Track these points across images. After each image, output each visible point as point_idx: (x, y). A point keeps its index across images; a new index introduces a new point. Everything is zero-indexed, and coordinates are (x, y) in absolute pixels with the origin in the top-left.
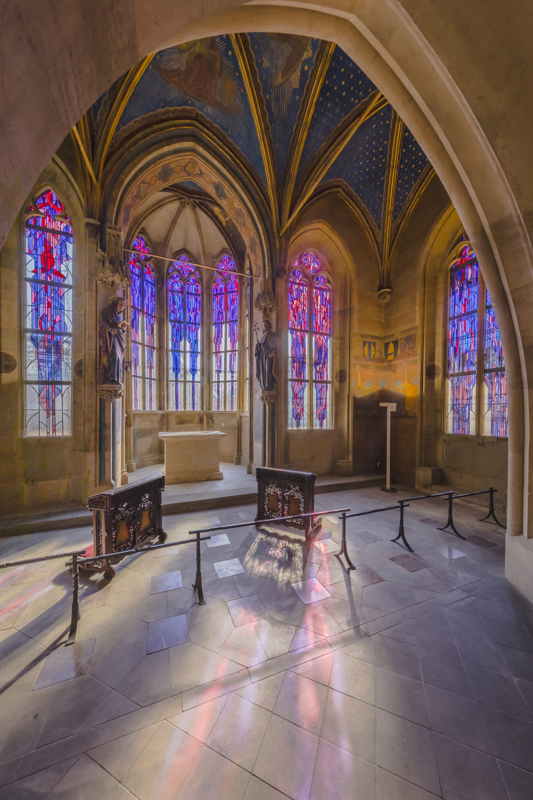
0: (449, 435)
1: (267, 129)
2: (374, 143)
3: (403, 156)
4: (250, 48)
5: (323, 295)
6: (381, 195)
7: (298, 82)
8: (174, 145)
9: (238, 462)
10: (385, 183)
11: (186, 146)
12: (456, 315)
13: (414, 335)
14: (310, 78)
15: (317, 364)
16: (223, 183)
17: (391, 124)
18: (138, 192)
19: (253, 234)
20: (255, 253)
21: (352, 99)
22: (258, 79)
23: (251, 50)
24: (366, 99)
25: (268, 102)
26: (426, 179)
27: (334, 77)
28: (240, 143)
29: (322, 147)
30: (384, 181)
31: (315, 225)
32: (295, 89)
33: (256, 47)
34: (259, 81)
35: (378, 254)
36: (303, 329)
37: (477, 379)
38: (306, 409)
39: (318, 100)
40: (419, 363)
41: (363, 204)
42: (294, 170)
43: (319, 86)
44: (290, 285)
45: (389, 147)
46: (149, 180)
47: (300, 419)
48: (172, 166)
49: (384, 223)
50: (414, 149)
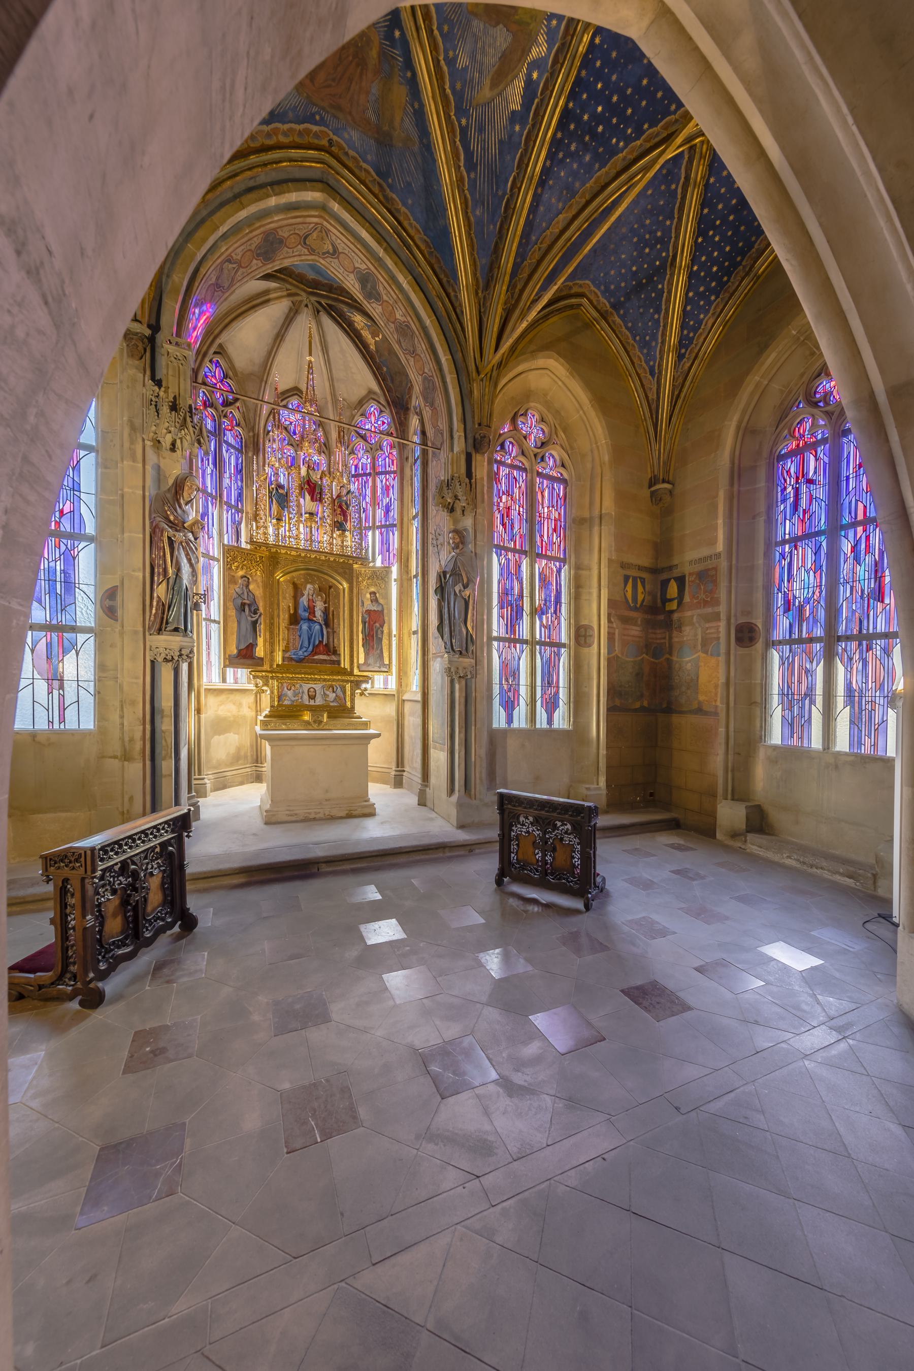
1: (460, 180)
2: (648, 222)
3: (697, 249)
4: (435, 28)
6: (656, 316)
7: (519, 99)
8: (287, 195)
9: (398, 782)
11: (309, 199)
14: (541, 94)
16: (376, 272)
17: (679, 190)
18: (217, 279)
19: (430, 370)
21: (614, 140)
22: (447, 86)
23: (436, 32)
24: (638, 143)
25: (464, 131)
27: (585, 96)
28: (410, 202)
29: (558, 223)
30: (662, 290)
31: (541, 362)
32: (513, 112)
33: (446, 28)
34: (448, 91)
39: (554, 134)
41: (624, 329)
42: (508, 260)
44: (495, 466)
45: (673, 231)
49: (660, 365)
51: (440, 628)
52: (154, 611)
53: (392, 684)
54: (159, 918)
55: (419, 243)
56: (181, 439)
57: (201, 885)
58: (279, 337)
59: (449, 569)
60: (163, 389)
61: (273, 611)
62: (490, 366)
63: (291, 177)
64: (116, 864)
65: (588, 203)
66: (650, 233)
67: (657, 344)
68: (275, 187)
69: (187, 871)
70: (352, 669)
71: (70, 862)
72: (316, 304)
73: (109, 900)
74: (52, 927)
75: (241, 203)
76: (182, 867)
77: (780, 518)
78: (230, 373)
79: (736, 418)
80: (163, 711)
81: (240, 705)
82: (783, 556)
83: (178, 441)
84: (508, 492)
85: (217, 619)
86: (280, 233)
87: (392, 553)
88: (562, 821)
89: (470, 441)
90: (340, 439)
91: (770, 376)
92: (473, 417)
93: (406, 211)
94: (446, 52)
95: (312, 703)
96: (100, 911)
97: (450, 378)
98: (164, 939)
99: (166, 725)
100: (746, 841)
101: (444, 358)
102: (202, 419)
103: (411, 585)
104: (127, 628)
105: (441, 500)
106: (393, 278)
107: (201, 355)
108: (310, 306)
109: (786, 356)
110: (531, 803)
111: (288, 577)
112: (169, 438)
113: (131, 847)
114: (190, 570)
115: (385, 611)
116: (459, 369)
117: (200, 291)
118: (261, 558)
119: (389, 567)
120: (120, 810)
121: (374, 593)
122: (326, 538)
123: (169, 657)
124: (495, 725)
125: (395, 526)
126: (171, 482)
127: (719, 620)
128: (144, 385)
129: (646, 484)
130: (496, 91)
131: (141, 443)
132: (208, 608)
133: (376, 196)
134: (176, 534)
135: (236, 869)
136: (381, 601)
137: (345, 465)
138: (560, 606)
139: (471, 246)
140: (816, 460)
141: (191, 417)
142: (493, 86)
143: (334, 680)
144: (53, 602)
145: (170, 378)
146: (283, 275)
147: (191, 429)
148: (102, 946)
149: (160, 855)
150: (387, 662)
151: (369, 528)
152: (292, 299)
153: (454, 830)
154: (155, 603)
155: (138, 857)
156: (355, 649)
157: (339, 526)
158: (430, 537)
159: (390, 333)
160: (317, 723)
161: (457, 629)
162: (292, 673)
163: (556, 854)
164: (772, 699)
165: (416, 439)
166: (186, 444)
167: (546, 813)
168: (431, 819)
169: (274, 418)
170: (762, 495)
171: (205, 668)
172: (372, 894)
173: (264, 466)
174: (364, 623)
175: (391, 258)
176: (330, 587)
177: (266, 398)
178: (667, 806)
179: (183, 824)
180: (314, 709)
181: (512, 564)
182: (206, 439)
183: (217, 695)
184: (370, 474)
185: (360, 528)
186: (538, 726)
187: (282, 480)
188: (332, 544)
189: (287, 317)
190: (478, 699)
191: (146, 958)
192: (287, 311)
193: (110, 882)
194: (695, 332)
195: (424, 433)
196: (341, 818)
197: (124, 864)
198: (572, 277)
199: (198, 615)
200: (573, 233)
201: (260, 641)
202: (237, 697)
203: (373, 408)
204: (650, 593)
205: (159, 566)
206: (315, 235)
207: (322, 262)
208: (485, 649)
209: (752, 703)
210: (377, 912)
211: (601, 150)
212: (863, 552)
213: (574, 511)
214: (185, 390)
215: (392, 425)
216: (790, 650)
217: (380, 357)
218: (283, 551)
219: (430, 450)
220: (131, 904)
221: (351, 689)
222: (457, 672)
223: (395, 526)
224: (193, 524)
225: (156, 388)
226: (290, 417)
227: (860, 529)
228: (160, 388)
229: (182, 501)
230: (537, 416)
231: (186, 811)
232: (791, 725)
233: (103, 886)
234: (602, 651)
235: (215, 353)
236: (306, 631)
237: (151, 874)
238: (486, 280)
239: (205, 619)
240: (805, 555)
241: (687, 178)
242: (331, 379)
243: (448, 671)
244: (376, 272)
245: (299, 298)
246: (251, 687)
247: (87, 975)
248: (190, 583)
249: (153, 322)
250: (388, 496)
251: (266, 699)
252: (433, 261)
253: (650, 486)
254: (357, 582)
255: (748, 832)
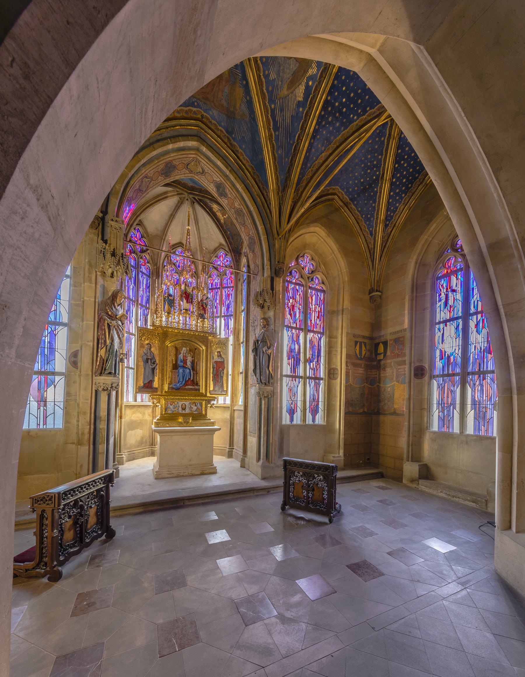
0: (435, 433)
1: (271, 136)
2: (369, 156)
3: (395, 171)
5: (318, 295)
6: (374, 205)
7: (302, 95)
8: (178, 143)
9: (230, 455)
10: (378, 194)
12: (442, 320)
13: (404, 337)
15: (310, 361)
16: (225, 183)
17: (386, 141)
18: (140, 186)
20: (253, 252)
21: (352, 116)
22: (264, 89)
24: (364, 117)
25: (273, 111)
26: (416, 193)
27: (336, 94)
28: (244, 146)
29: (322, 157)
31: (312, 229)
32: (299, 102)
34: (265, 91)
35: (369, 259)
36: (298, 327)
37: (461, 381)
38: (299, 404)
39: (320, 113)
40: (407, 362)
41: (356, 211)
43: (322, 101)
44: (287, 284)
45: (383, 161)
46: (151, 175)
47: (294, 413)
48: (176, 163)
49: (375, 230)
50: (405, 165)
51: (255, 371)
52: (98, 363)
53: (228, 401)
54: (94, 531)
55: (248, 167)
56: (117, 271)
57: (119, 513)
58: (172, 216)
59: (260, 339)
60: (108, 245)
61: (164, 362)
62: (285, 231)
63: (181, 134)
64: (72, 502)
65: (338, 147)
66: (370, 162)
67: (374, 219)
68: (172, 139)
69: (111, 506)
70: (206, 393)
71: (46, 501)
72: (193, 199)
73: (66, 521)
74: (35, 538)
75: (154, 148)
76: (108, 503)
77: (438, 310)
78: (145, 235)
79: (415, 258)
80: (101, 418)
81: (144, 414)
82: (439, 330)
83: (115, 272)
84: (293, 297)
85: (133, 367)
86: (174, 163)
87: (228, 330)
88: (318, 474)
89: (273, 271)
90: (203, 270)
91: (433, 235)
92: (275, 258)
93: (242, 151)
94: (264, 71)
95: (184, 412)
96: (61, 528)
97: (263, 238)
98: (97, 542)
99: (102, 425)
100: (418, 484)
101: (260, 227)
102: (128, 261)
103: (240, 348)
104: (83, 373)
105: (257, 302)
106: (234, 186)
107: (130, 226)
108: (189, 200)
109: (441, 225)
110: (301, 465)
111: (173, 344)
112: (110, 271)
113: (80, 492)
114: (119, 341)
115: (225, 362)
116: (269, 233)
117: (130, 193)
118: (158, 333)
119: (228, 338)
120: (75, 472)
121: (219, 352)
122: (194, 322)
123: (105, 388)
124: (284, 423)
125: (232, 315)
126: (110, 294)
127: (405, 364)
128: (98, 243)
129: (367, 292)
130: (290, 91)
131: (95, 273)
132: (128, 361)
133: (225, 143)
134: (112, 322)
135: (138, 504)
136: (223, 356)
137: (206, 284)
138: (320, 358)
139: (276, 169)
140: (457, 279)
141: (123, 259)
142: (289, 88)
143: (196, 399)
144: (43, 359)
145: (112, 239)
146: (176, 184)
147: (122, 266)
148: (62, 547)
149: (96, 496)
150: (225, 389)
151: (218, 317)
152: (179, 196)
153: (260, 480)
154: (99, 359)
155: (84, 498)
156: (208, 381)
157: (202, 316)
158: (251, 321)
159: (231, 214)
160: (187, 423)
161: (264, 371)
162: (173, 396)
163: (314, 492)
164: (433, 406)
165: (245, 269)
166: (119, 274)
167: (309, 470)
168: (248, 475)
169: (168, 259)
170: (428, 299)
171: (125, 394)
172: (213, 516)
173: (162, 284)
174: (213, 368)
175: (233, 176)
176: (196, 349)
177: (164, 249)
178: (376, 465)
179: (109, 479)
180: (184, 415)
181: (294, 335)
182: (130, 271)
183: (131, 409)
184: (219, 288)
185: (213, 317)
186: (307, 423)
187: (171, 292)
188: (197, 326)
189: (177, 206)
190: (274, 409)
191: (86, 554)
192: (177, 203)
193: (68, 511)
194: (394, 213)
195: (248, 266)
196: (198, 475)
197: (76, 501)
198: (329, 184)
199: (122, 365)
200: (330, 162)
201: (156, 379)
202: (142, 409)
203: (221, 253)
204: (369, 350)
205: (102, 339)
206: (193, 163)
207: (196, 178)
208: (279, 382)
209: (422, 409)
210: (215, 526)
211: (345, 120)
212: (481, 327)
213: (328, 307)
214: (120, 245)
215: (232, 262)
216: (443, 381)
217: (226, 226)
218: (170, 330)
219: (252, 276)
220: (79, 524)
221: (206, 404)
222: (263, 394)
223: (232, 315)
224: (122, 316)
225: (104, 244)
226: (177, 259)
227: (479, 316)
228: (106, 245)
229: (116, 304)
230: (309, 257)
231: (111, 472)
232: (443, 420)
233: (64, 514)
234: (342, 382)
235: (137, 224)
236: (181, 372)
237: (91, 507)
238: (283, 187)
239: (126, 367)
240: (450, 329)
241: (390, 134)
242: (200, 238)
243: (258, 393)
244: (225, 183)
245: (183, 196)
246: (150, 404)
247: (53, 563)
248: (118, 348)
249: (104, 210)
250: (229, 300)
251: (158, 411)
252: (255, 177)
253: (370, 294)
254: (211, 346)
255: (420, 478)
